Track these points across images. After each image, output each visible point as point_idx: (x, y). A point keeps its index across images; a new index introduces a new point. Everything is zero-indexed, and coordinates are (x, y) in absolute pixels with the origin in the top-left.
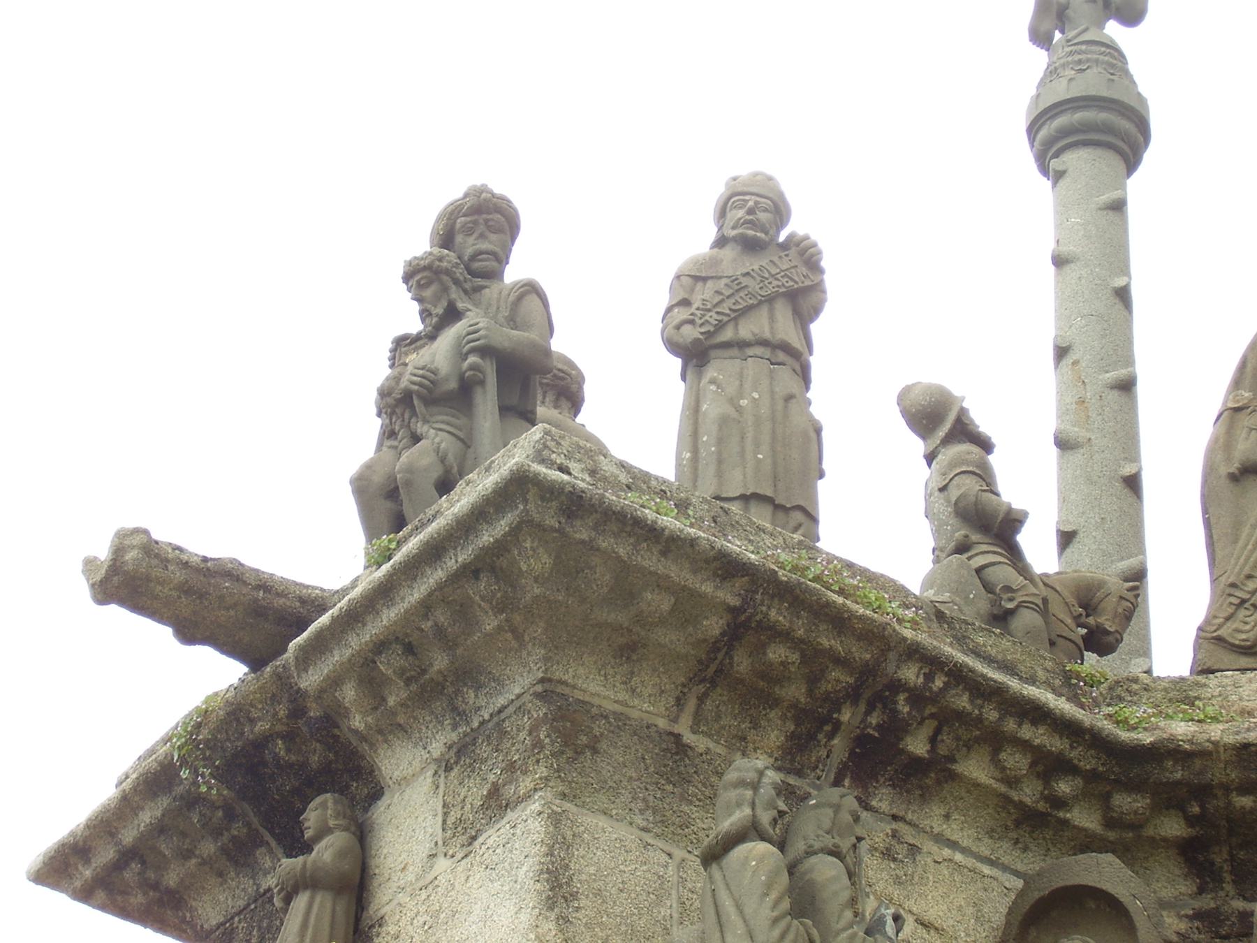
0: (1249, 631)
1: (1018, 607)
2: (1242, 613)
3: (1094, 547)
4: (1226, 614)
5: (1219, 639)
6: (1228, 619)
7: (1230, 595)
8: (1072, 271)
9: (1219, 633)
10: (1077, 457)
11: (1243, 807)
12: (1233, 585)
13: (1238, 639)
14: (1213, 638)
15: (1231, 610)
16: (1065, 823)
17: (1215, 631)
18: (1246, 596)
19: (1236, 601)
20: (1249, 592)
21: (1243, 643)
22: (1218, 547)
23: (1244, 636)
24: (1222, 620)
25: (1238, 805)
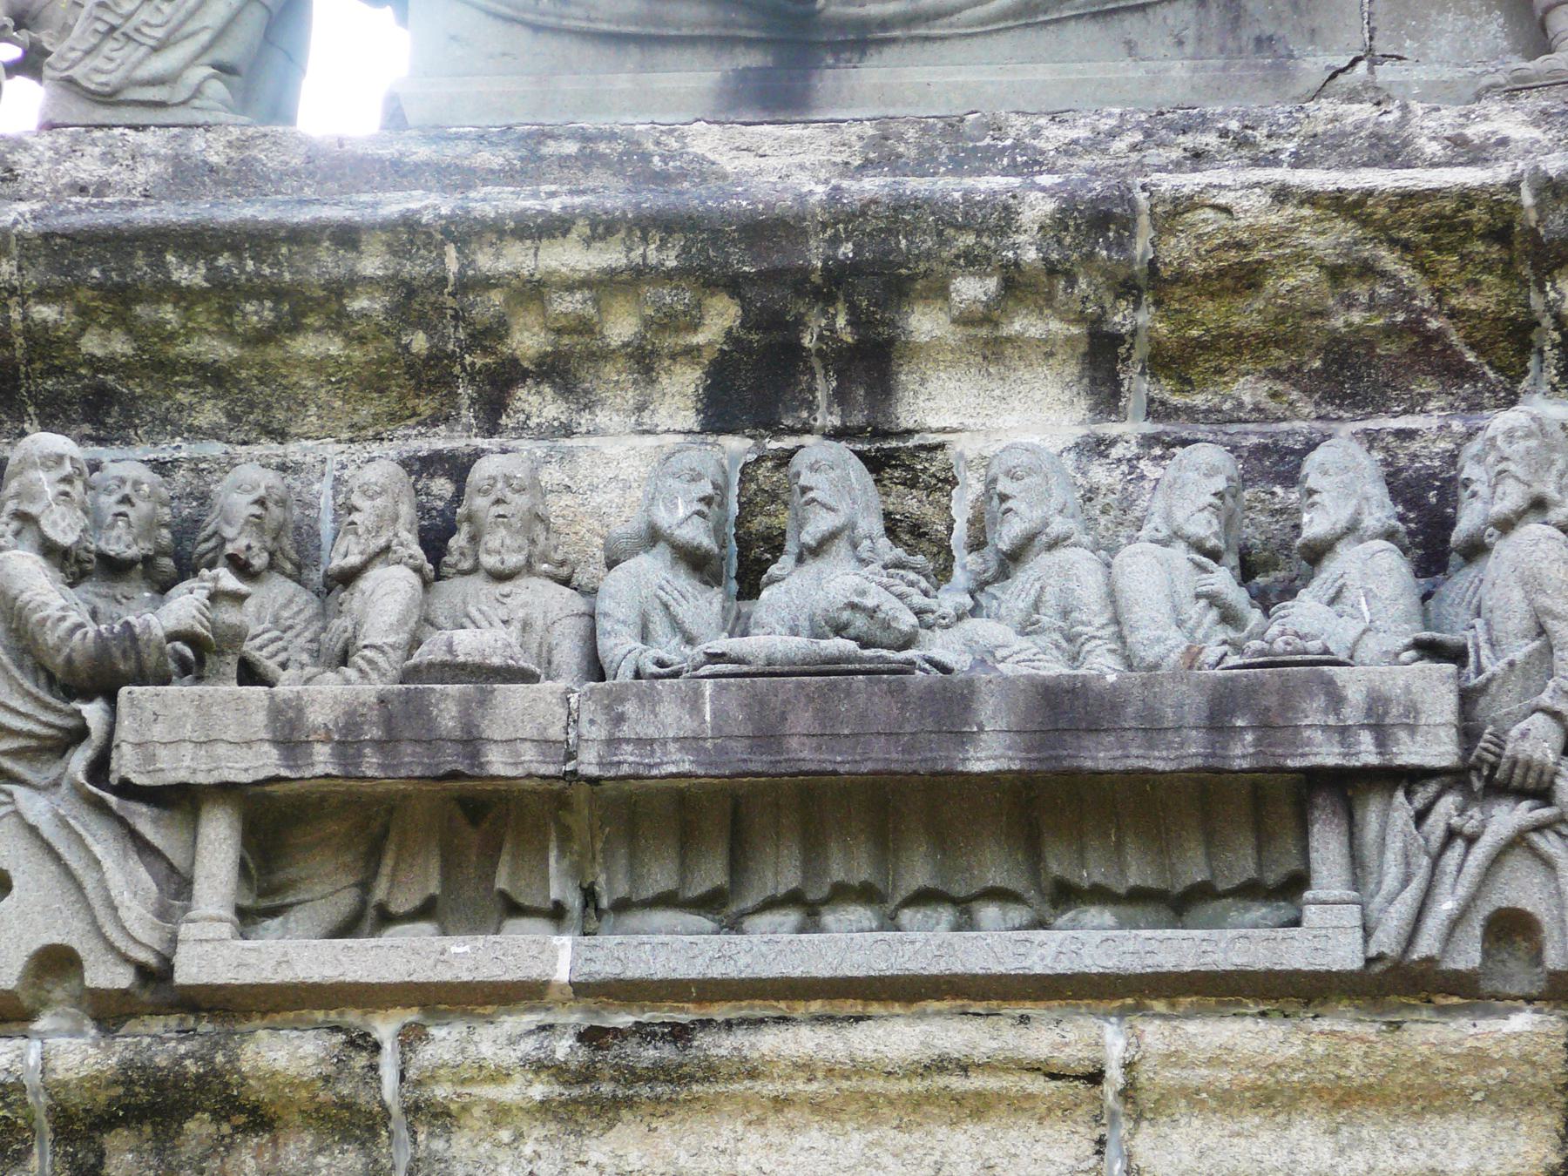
0: (112, 72)
2: (110, 45)
4: (85, 46)
5: (70, 81)
6: (88, 53)
7: (98, 19)
9: (70, 73)
11: (45, 321)
13: (94, 82)
14: (63, 79)
15: (94, 40)
17: (67, 69)
18: (115, 21)
19: (102, 27)
20: (121, 16)
21: (100, 89)
23: (103, 78)
24: (78, 54)
25: (36, 316)
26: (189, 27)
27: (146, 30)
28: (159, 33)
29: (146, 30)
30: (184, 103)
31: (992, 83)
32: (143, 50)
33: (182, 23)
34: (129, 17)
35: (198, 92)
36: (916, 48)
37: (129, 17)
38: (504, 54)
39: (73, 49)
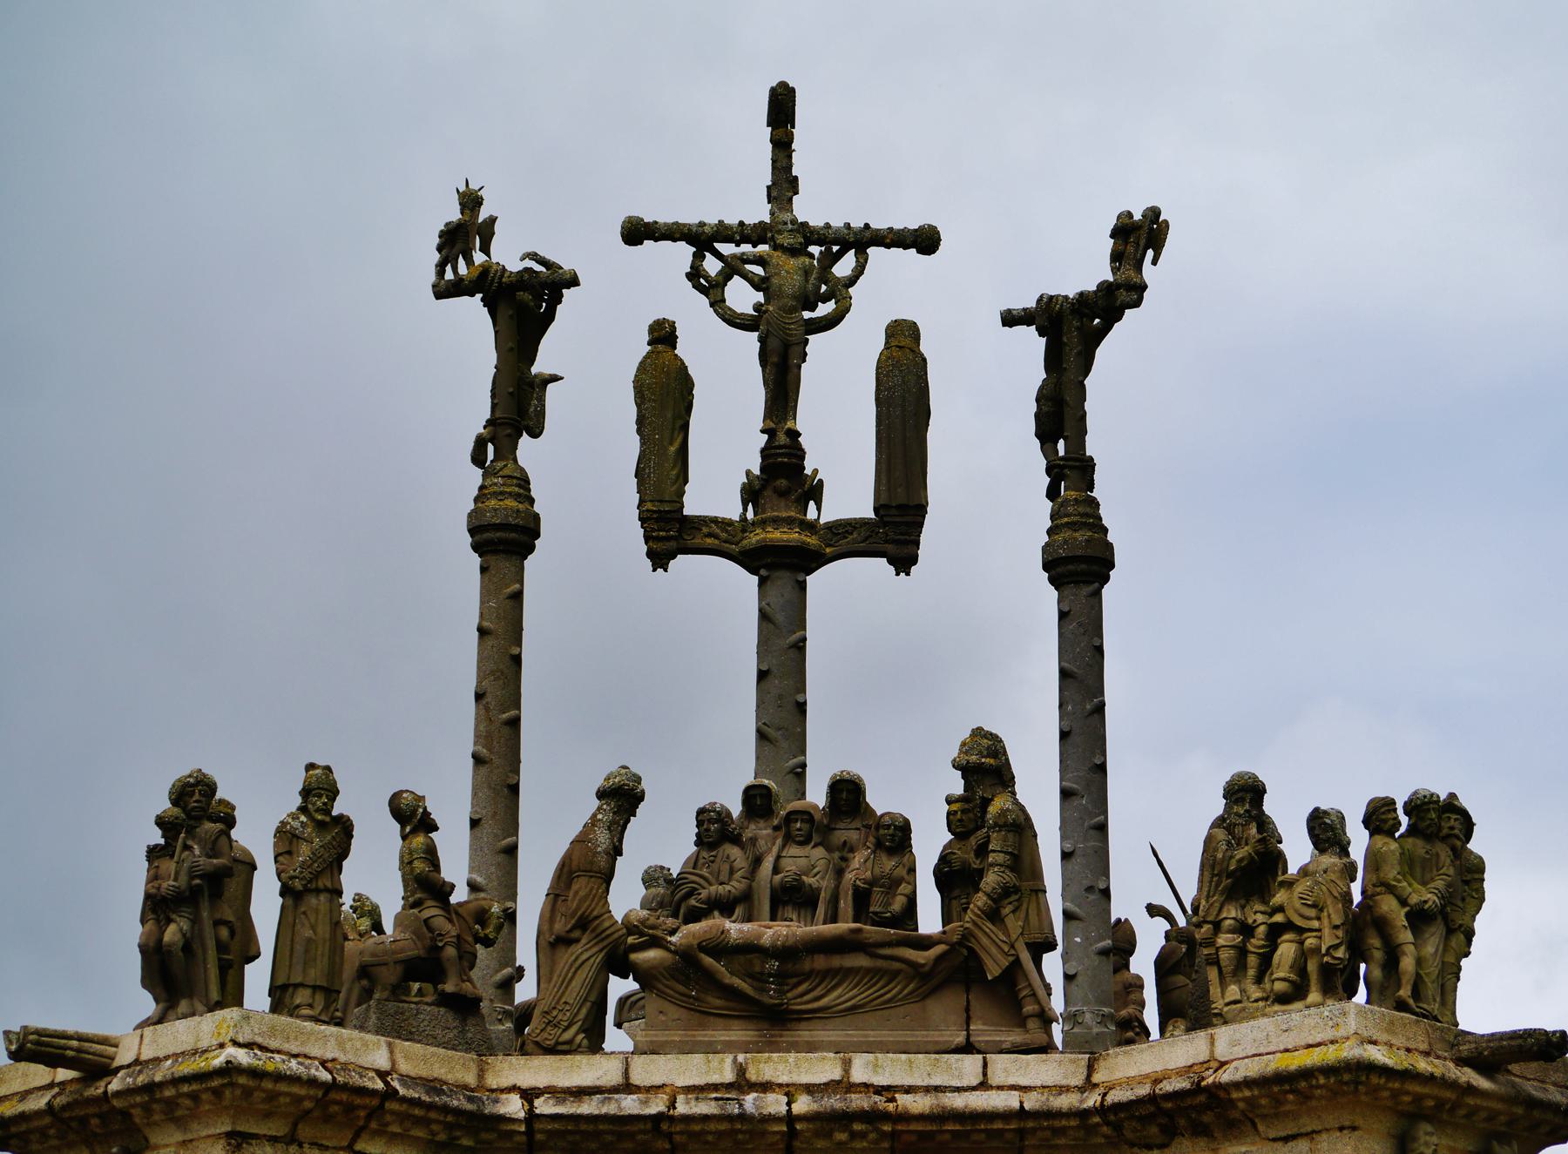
1: (446, 944)
2: (549, 1028)
3: (490, 830)
6: (542, 1031)
7: (544, 1017)
8: (490, 641)
10: (484, 770)
12: (546, 1012)
15: (544, 1026)
16: (459, 1145)
18: (552, 1019)
19: (547, 1021)
22: (542, 981)
23: (548, 1043)
24: (538, 1031)
26: (575, 1020)
27: (562, 1023)
28: (566, 1024)
29: (562, 1023)
30: (575, 1050)
31: (844, 1041)
32: (561, 1030)
33: (574, 1018)
34: (555, 1018)
35: (579, 1046)
36: (817, 1021)
37: (555, 1018)
38: (679, 1020)
39: (536, 1028)
